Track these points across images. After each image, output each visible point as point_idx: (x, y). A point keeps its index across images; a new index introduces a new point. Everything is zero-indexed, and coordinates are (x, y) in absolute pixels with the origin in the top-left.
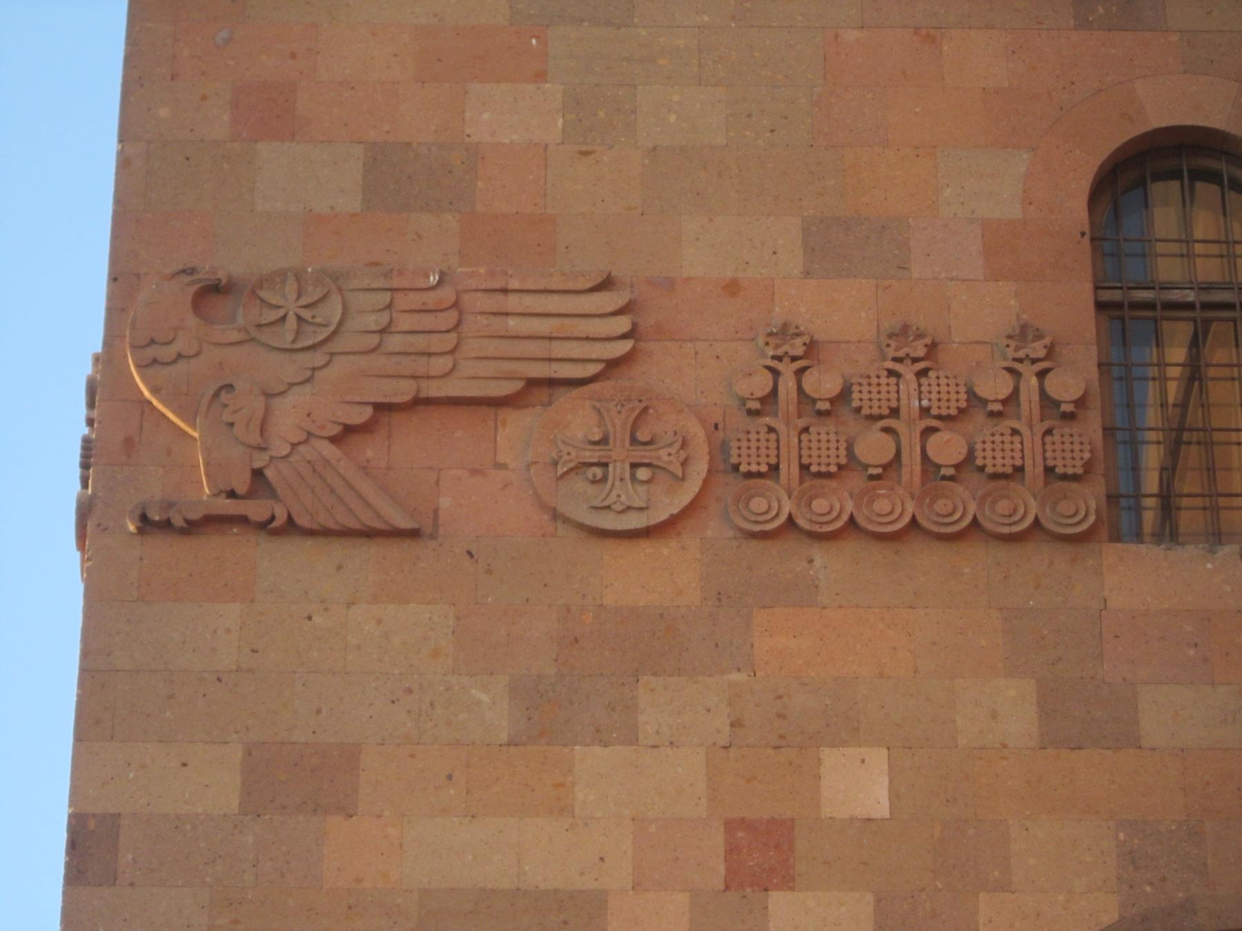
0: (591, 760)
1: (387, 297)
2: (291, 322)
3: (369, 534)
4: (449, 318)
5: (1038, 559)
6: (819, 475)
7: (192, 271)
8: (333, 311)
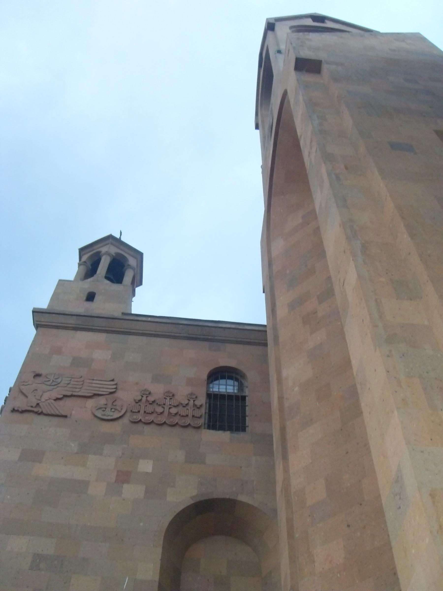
0: (92, 457)
2: (51, 381)
5: (189, 431)
6: (148, 413)
8: (59, 380)
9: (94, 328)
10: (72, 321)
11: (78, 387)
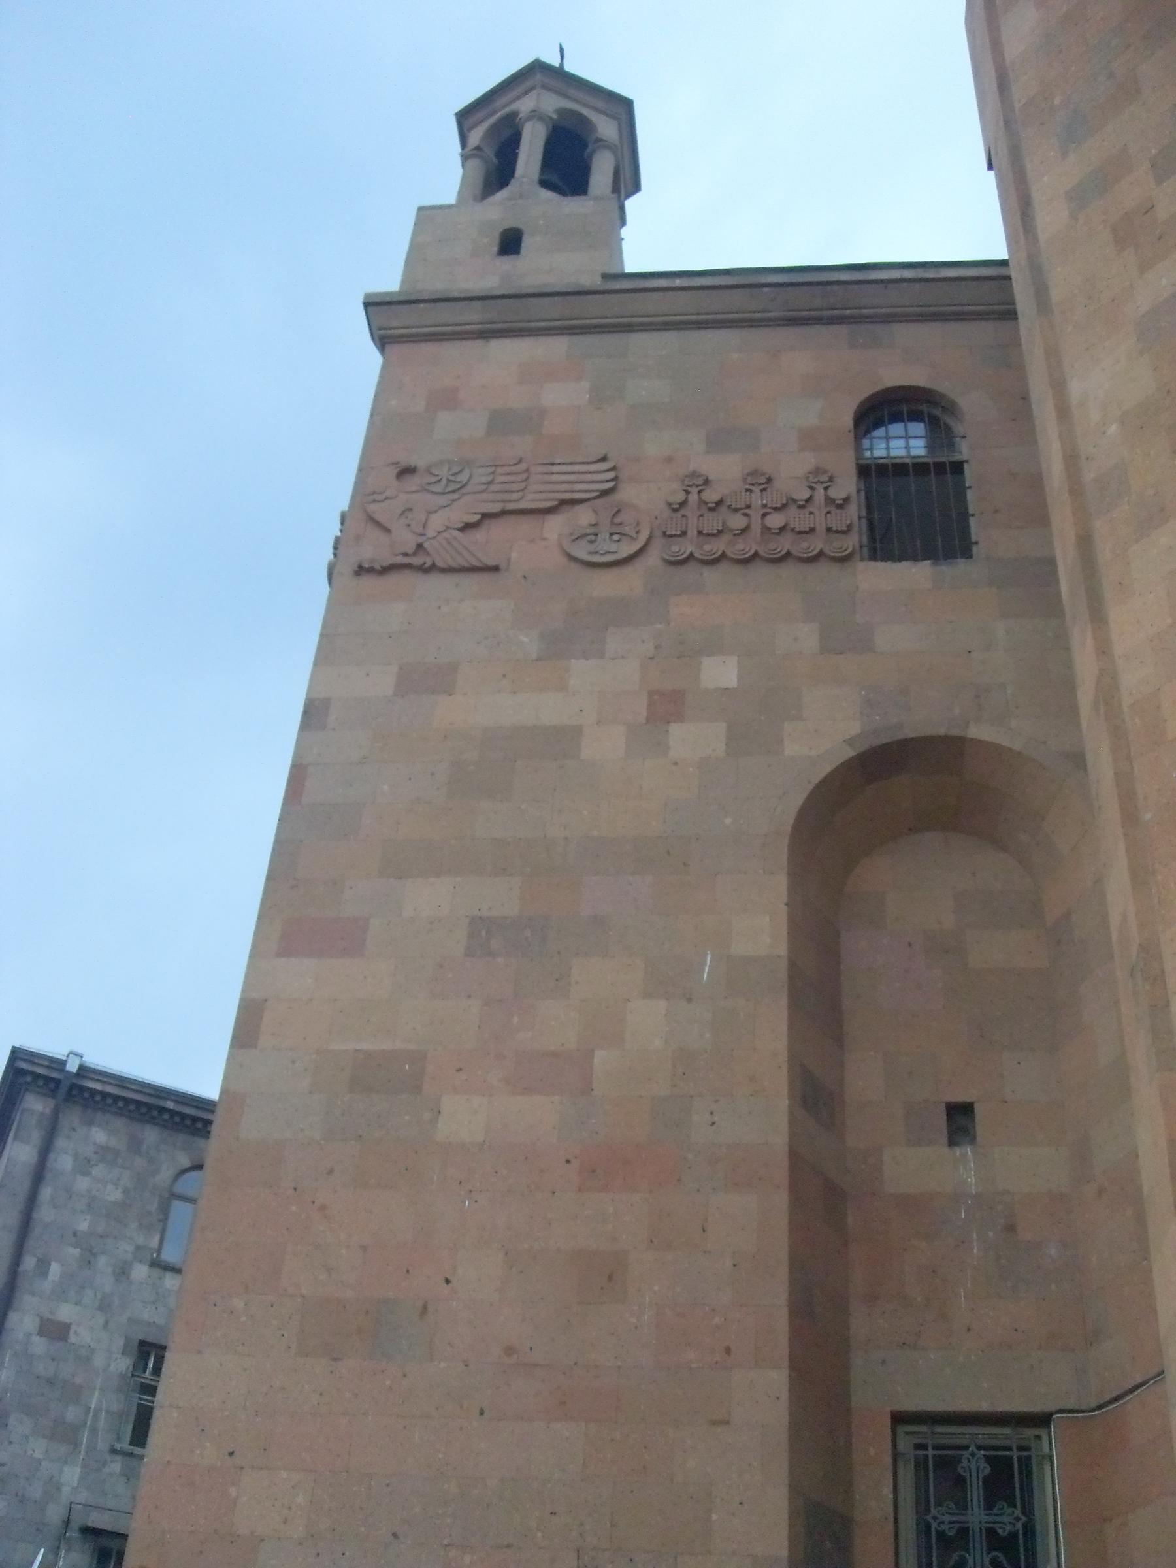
0: (578, 665)
1: (493, 469)
2: (444, 481)
3: (473, 569)
4: (524, 476)
5: (823, 568)
6: (708, 535)
7: (397, 463)
8: (463, 477)
9: (533, 325)
10: (472, 315)
11: (515, 487)
